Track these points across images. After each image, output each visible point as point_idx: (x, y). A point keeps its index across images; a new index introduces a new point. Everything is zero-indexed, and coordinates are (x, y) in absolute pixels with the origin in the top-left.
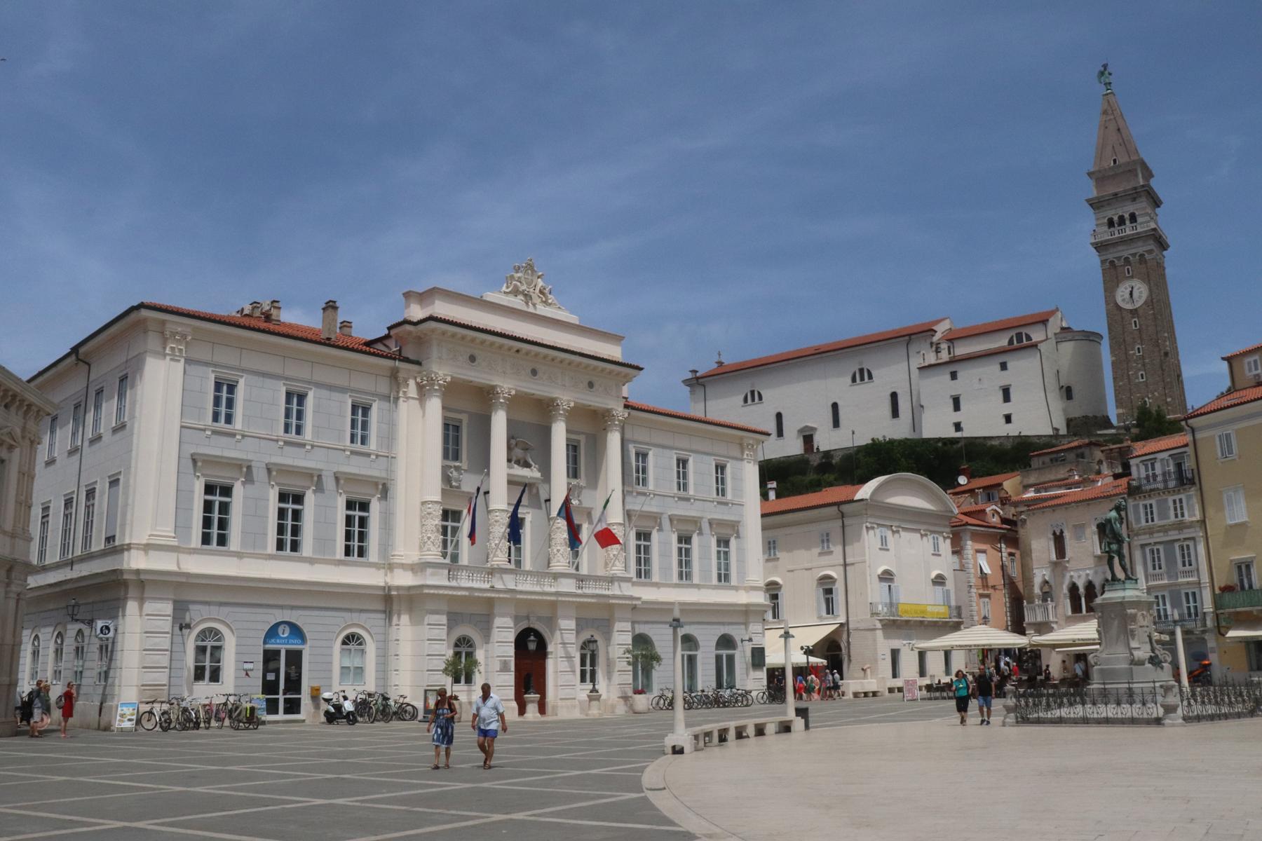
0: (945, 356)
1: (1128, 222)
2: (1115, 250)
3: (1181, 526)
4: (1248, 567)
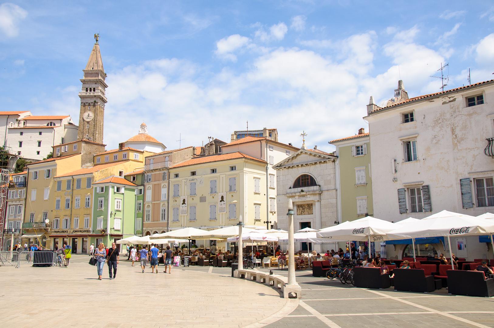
0: (22, 125)
1: (92, 91)
2: (86, 100)
3: (19, 200)
4: (33, 215)
